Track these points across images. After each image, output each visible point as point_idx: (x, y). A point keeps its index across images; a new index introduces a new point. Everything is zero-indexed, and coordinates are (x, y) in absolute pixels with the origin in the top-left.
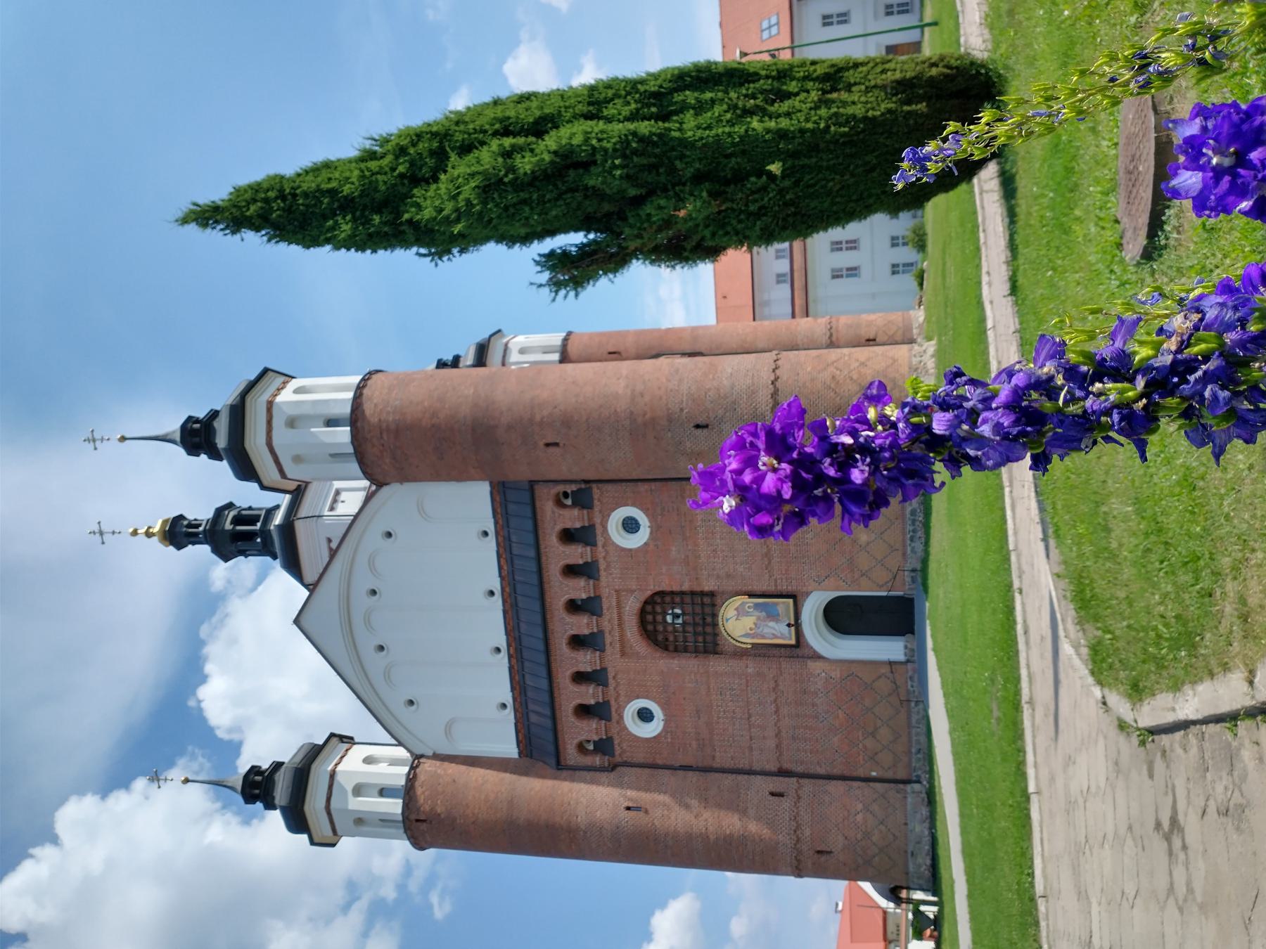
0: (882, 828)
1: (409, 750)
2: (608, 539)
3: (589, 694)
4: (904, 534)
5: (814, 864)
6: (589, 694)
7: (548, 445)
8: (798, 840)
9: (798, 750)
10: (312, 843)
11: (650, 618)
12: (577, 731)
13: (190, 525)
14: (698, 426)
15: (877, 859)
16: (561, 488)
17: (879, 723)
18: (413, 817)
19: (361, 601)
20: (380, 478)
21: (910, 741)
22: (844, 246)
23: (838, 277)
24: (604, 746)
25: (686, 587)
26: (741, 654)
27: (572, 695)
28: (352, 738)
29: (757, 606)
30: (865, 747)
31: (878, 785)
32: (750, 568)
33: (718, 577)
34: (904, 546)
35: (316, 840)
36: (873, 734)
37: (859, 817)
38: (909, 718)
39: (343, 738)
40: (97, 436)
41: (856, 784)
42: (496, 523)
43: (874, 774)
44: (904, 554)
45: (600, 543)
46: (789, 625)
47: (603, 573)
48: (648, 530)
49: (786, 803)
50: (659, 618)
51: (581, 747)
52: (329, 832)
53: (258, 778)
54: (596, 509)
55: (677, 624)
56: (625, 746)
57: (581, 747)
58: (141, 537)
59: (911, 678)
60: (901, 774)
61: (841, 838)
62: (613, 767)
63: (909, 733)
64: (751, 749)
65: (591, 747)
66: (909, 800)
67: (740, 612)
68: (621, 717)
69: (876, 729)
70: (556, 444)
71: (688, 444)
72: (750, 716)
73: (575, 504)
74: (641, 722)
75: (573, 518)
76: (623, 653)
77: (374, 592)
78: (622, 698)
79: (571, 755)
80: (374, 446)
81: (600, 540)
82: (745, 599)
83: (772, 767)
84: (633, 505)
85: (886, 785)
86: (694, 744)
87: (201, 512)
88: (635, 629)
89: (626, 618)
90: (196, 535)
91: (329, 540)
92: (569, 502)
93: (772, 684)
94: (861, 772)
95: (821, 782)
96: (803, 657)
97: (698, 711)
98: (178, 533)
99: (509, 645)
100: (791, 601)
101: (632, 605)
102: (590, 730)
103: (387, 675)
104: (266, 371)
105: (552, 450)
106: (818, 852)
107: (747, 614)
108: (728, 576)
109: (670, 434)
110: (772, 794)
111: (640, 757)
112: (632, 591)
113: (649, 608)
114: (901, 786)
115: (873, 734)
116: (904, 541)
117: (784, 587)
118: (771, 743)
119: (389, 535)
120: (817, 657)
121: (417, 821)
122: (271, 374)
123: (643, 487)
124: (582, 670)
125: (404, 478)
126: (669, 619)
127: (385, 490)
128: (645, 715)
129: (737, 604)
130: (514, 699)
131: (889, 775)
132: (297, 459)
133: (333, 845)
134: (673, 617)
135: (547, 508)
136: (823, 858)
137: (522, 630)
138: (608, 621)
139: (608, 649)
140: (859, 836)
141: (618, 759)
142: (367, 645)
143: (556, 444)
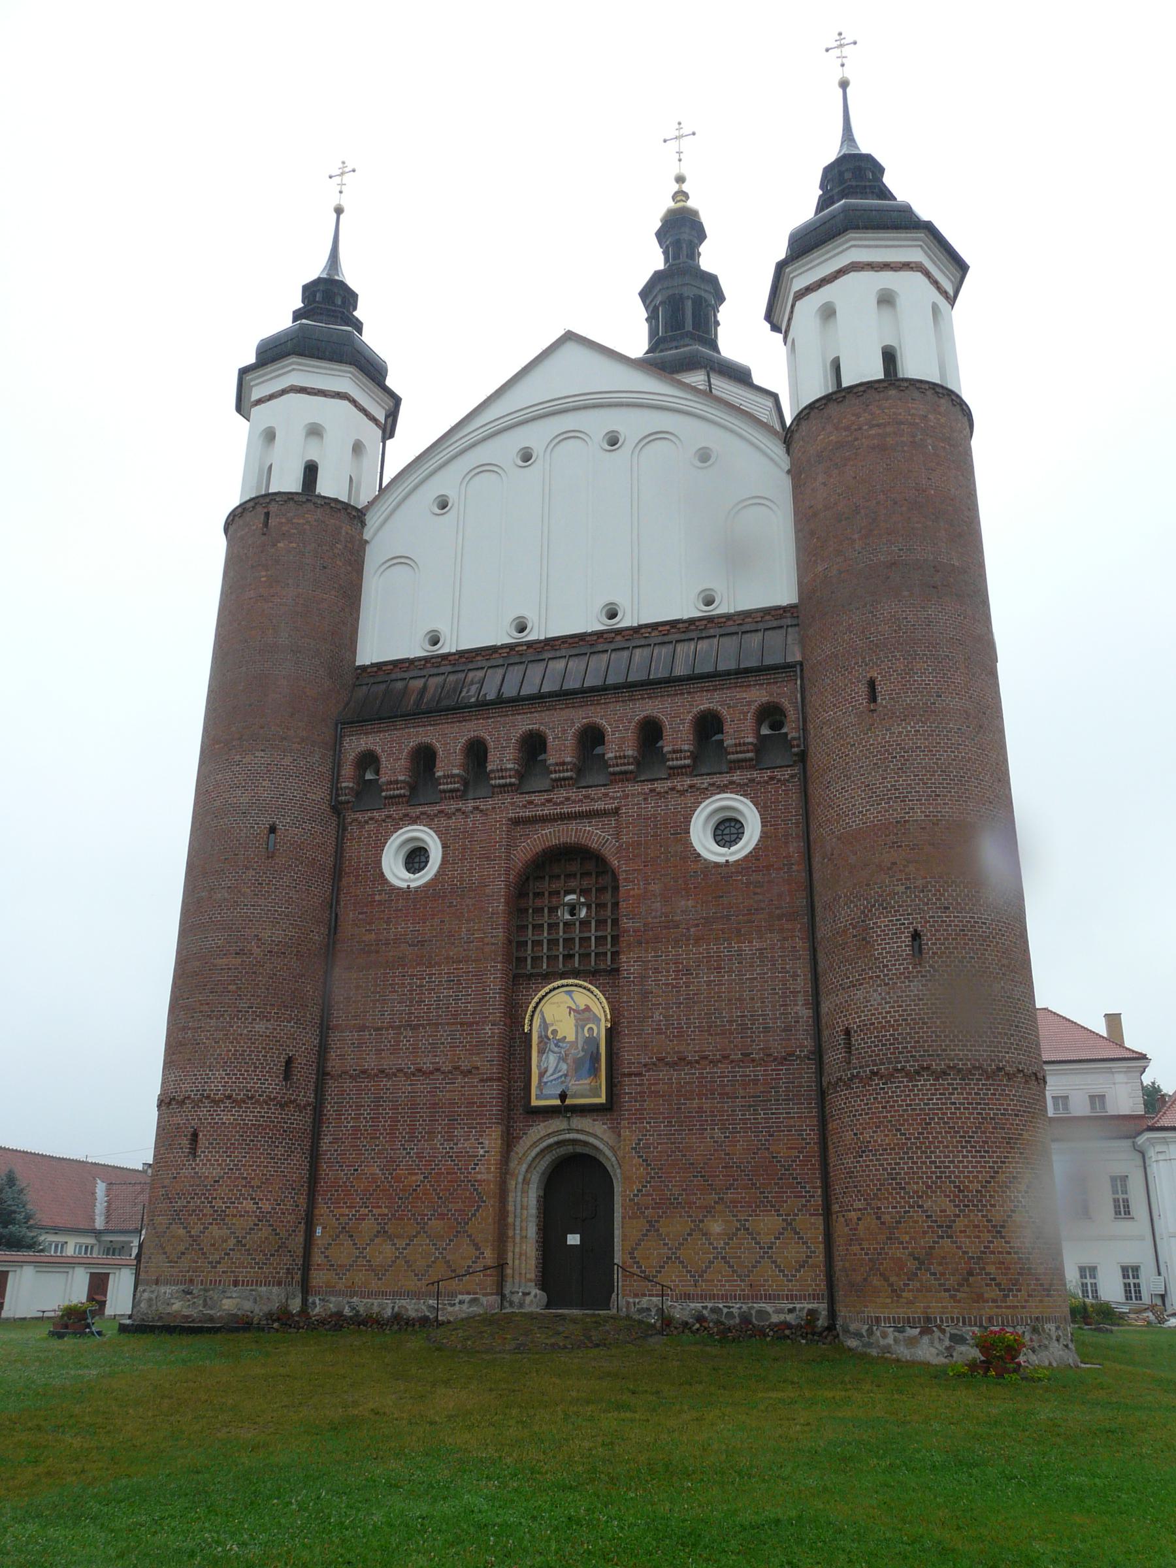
0: (232, 1242)
1: (371, 504)
2: (705, 793)
3: (450, 764)
4: (724, 1297)
6: (450, 764)
7: (872, 684)
8: (216, 1102)
9: (359, 1107)
10: (243, 372)
11: (574, 867)
12: (393, 749)
14: (916, 936)
15: (182, 1232)
16: (792, 714)
17: (400, 1243)
18: (273, 508)
21: (370, 1295)
22: (1121, 1196)
23: (1114, 1186)
24: (366, 791)
25: (626, 923)
26: (514, 1015)
27: (449, 742)
28: (392, 435)
29: (592, 1041)
30: (362, 1218)
31: (301, 1239)
32: (659, 1031)
33: (643, 978)
34: (703, 1298)
35: (248, 377)
36: (382, 1233)
37: (248, 1205)
39: (393, 415)
40: (847, 50)
41: (303, 1200)
43: (319, 1230)
44: (688, 1297)
45: (697, 781)
46: (563, 1096)
47: (647, 787)
48: (722, 860)
49: (273, 1086)
50: (573, 884)
51: (369, 760)
52: (255, 396)
53: (339, 301)
54: (755, 774)
55: (561, 907)
56: (371, 826)
57: (369, 760)
58: (675, 187)
59: (474, 1301)
60: (318, 1278)
61: (216, 1172)
62: (337, 809)
63: (384, 1294)
64: (362, 1028)
65: (369, 776)
66: (275, 1290)
67: (583, 1015)
68: (414, 821)
70: (873, 697)
71: (883, 921)
72: (415, 1028)
73: (762, 739)
74: (406, 857)
75: (740, 730)
76: (517, 822)
77: (613, 441)
78: (444, 821)
79: (356, 745)
80: (858, 416)
81: (704, 782)
82: (604, 1025)
83: (334, 1064)
84: (764, 836)
85: (300, 1252)
87: (709, 259)
88: (555, 842)
89: (573, 825)
92: (765, 731)
93: (465, 1065)
94: (322, 1209)
95: (307, 1144)
96: (509, 1118)
98: (681, 231)
99: (530, 645)
100: (602, 1100)
101: (594, 834)
102: (395, 767)
104: (962, 267)
105: (863, 689)
106: (195, 1135)
107: (579, 1026)
108: (645, 995)
109: (901, 889)
110: (289, 1061)
111: (354, 851)
112: (617, 836)
113: (590, 866)
114: (298, 1277)
116: (713, 1297)
117: (628, 1087)
118: (371, 1062)
120: (509, 1142)
121: (267, 515)
122: (959, 275)
123: (794, 848)
124: (490, 757)
125: (798, 475)
126: (569, 898)
127: (777, 450)
128: (416, 858)
129: (597, 1009)
130: (445, 657)
131: (317, 1258)
132: (828, 313)
133: (239, 409)
134: (573, 903)
135: (758, 695)
136: (185, 1142)
137: (551, 664)
138: (569, 799)
139: (520, 800)
140: (218, 1204)
141: (350, 816)
143: (873, 697)
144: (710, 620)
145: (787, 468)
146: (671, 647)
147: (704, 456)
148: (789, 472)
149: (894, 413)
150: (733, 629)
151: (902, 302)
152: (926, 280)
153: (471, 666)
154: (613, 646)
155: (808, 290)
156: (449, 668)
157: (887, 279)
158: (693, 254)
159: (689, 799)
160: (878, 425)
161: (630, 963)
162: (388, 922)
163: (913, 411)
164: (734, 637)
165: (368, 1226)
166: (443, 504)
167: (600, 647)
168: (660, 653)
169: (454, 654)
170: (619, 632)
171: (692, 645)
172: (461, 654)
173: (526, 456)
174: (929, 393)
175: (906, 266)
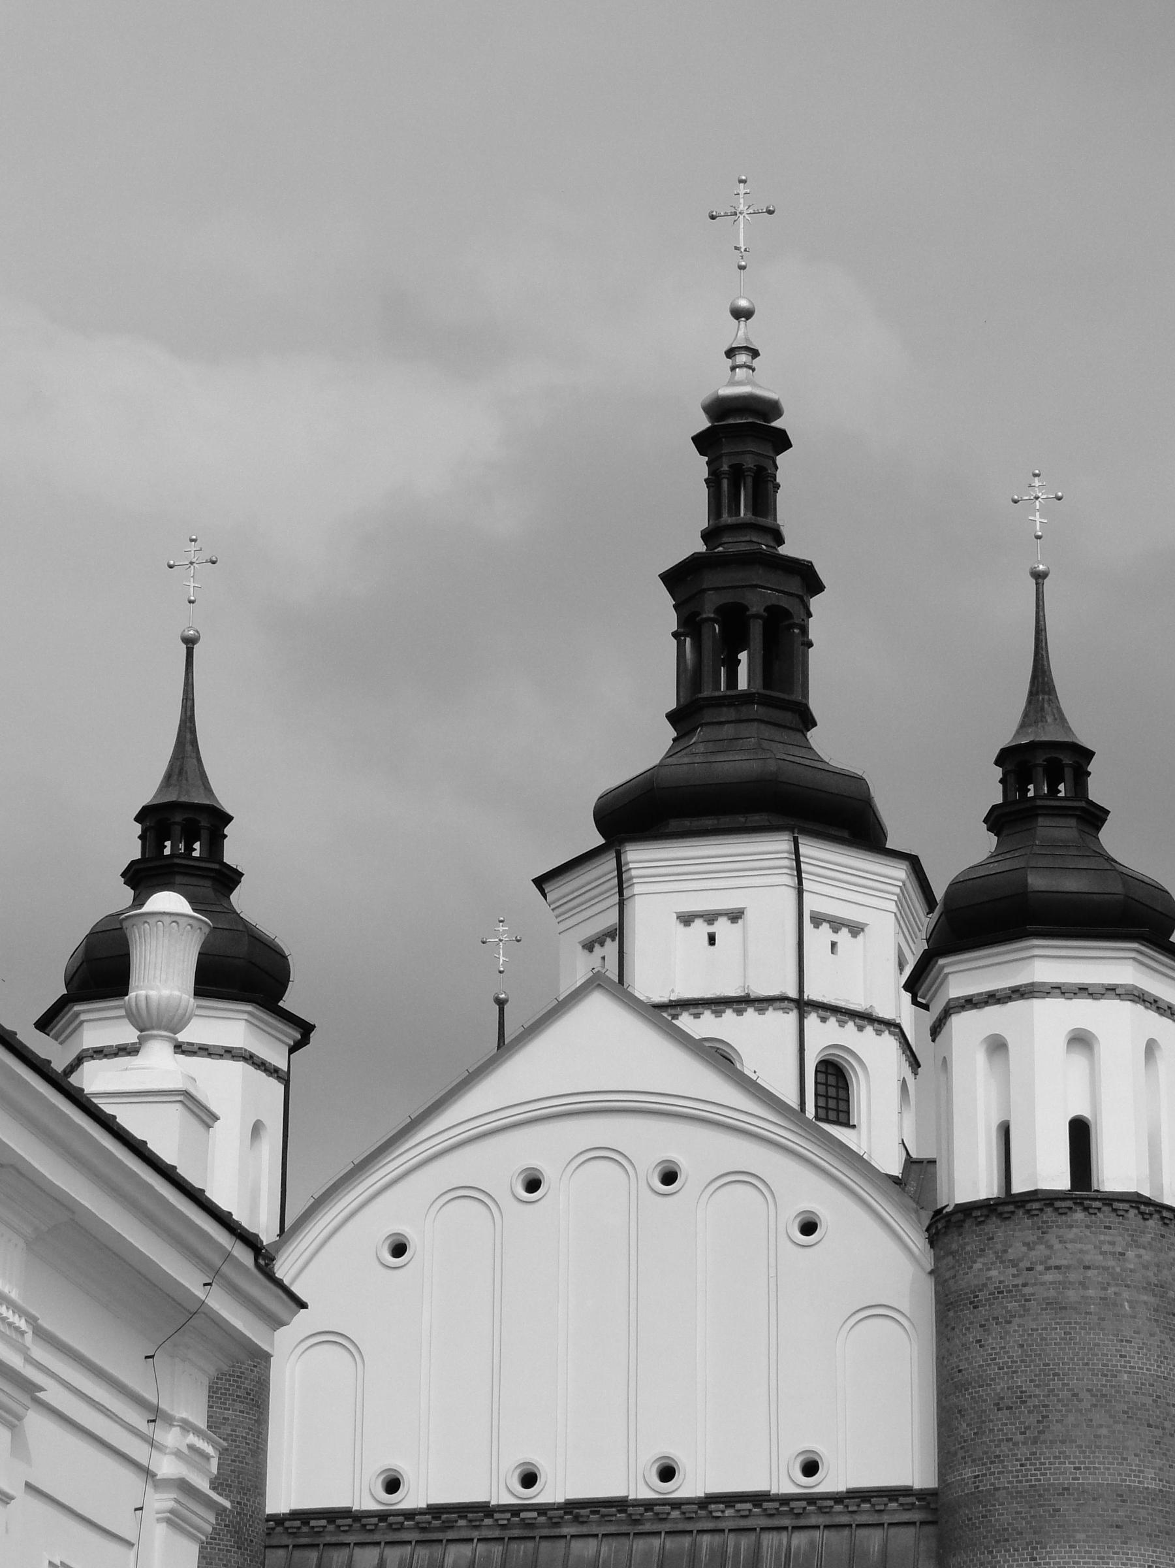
20: (953, 1242)
42: (838, 1498)
77: (669, 1177)
91: (735, 916)
119: (809, 1228)
127: (917, 1241)
132: (997, 1046)
144: (812, 1499)
145: (929, 1268)
146: (753, 1537)
148: (931, 1273)
149: (1081, 1251)
150: (844, 1519)
151: (1105, 1048)
152: (1140, 1008)
153: (451, 1535)
154: (667, 1526)
155: (970, 1003)
156: (414, 1536)
157: (1082, 1013)
158: (763, 488)
160: (1058, 1268)
163: (1106, 1248)
164: (846, 1532)
167: (647, 1527)
168: (737, 1548)
169: (422, 1512)
170: (677, 1504)
171: (784, 1536)
172: (436, 1511)
174: (1133, 1212)
175: (1111, 991)
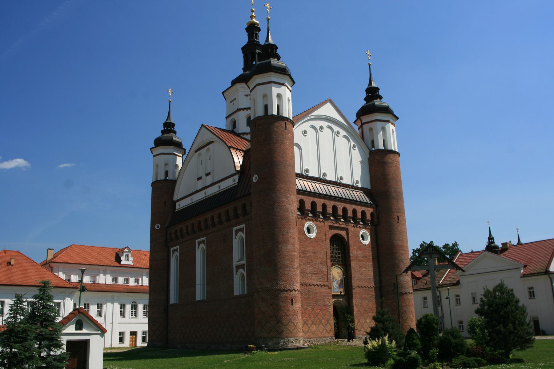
5: (287, 297)
13: (257, 34)
17: (317, 325)
19: (336, 128)
25: (351, 255)
38: (319, 337)
68: (309, 220)
69: (315, 324)
72: (315, 274)
74: (313, 229)
81: (361, 226)
86: (303, 249)
90: (253, 36)
97: (314, 253)
101: (343, 233)
102: (308, 206)
103: (313, 127)
106: (292, 300)
115: (313, 323)
127: (368, 152)
128: (309, 230)
136: (290, 301)
142: (325, 124)
147: (354, 146)
159: (359, 229)
161: (353, 264)
162: (307, 246)
165: (310, 322)
166: (305, 132)
173: (322, 128)
